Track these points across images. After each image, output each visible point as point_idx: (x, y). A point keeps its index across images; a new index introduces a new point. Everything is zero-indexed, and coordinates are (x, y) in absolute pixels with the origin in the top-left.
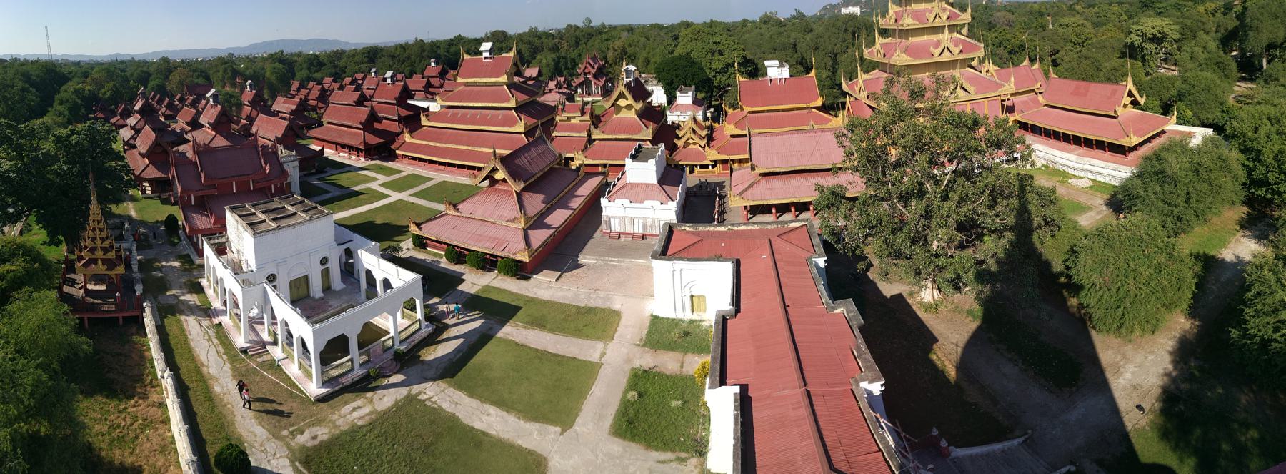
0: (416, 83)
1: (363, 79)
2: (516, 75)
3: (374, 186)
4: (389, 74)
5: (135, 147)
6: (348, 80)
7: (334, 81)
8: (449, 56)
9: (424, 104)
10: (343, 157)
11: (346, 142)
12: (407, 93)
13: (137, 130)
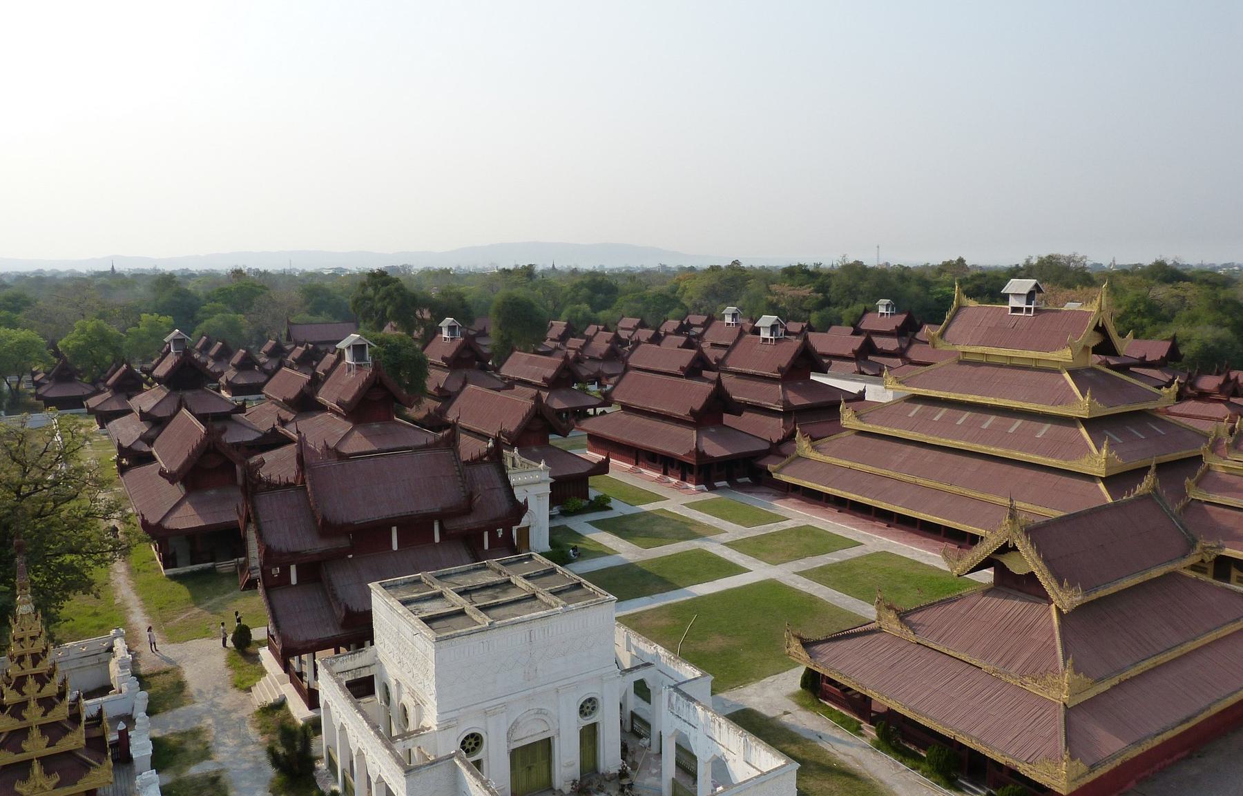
0: (838, 340)
1: (706, 325)
4: (766, 321)
5: (150, 458)
6: (672, 324)
7: (642, 325)
9: (853, 387)
10: (648, 479)
13: (156, 422)
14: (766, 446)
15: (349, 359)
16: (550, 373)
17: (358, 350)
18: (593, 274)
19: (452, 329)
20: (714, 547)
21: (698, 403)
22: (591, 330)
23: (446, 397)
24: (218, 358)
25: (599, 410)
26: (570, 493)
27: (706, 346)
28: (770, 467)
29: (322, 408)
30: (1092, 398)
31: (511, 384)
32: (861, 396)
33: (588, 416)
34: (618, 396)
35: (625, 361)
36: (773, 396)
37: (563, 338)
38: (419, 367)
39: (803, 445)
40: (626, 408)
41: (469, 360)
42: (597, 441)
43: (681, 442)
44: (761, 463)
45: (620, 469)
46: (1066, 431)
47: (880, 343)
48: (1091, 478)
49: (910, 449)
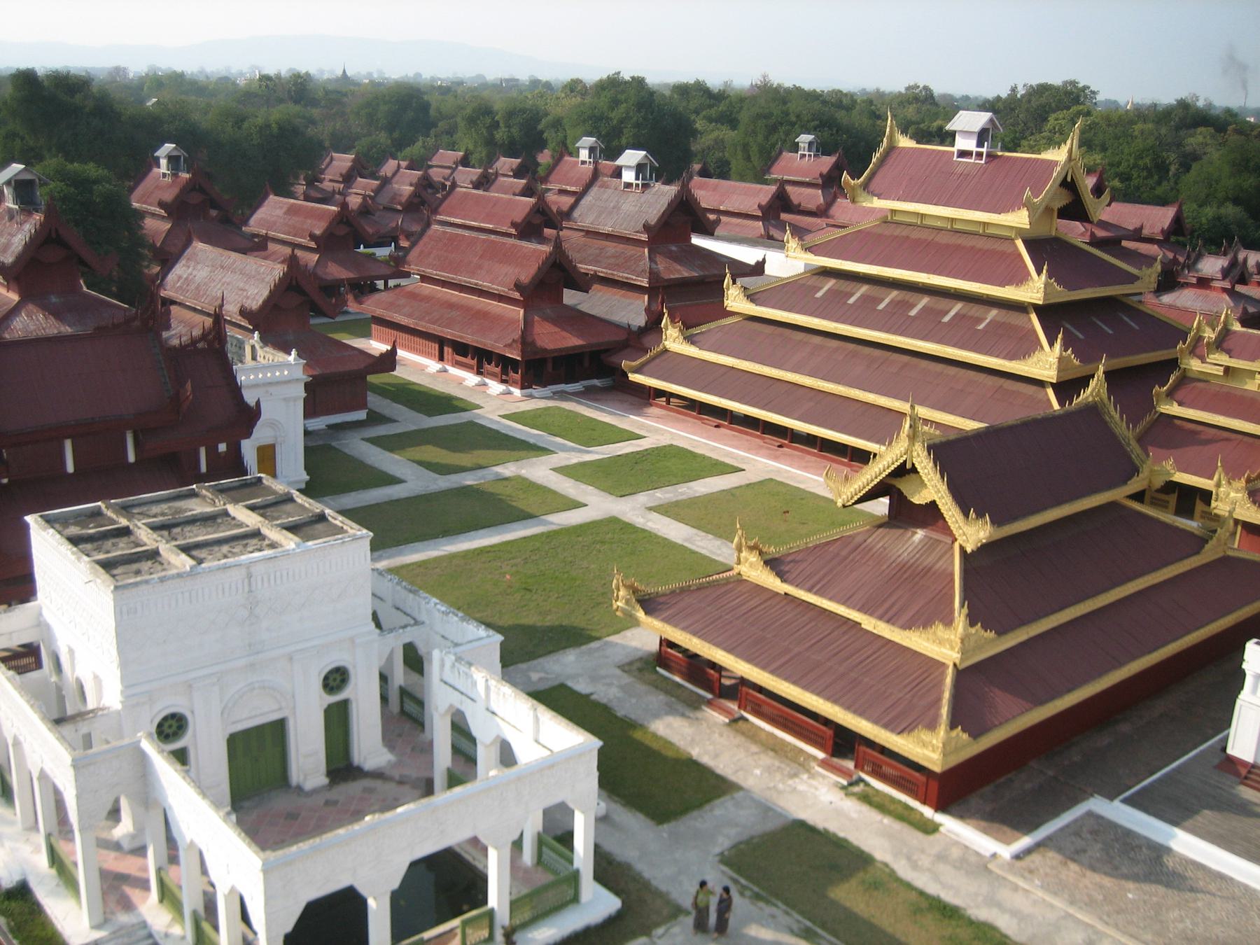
2: (1065, 213)
4: (632, 157)
8: (849, 134)
11: (469, 338)
12: (686, 217)
14: (622, 337)
20: (539, 471)
25: (391, 283)
28: (625, 364)
30: (1050, 276)
33: (374, 289)
37: (348, 179)
44: (614, 359)
46: (1015, 318)
48: (1040, 384)
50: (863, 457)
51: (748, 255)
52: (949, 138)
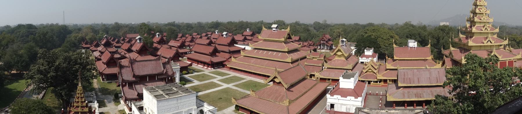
0: (238, 37)
1: (211, 34)
3: (215, 81)
6: (204, 34)
7: (198, 34)
8: (256, 29)
10: (200, 67)
14: (225, 60)
15: (138, 41)
16: (179, 45)
17: (140, 39)
18: (187, 24)
19: (158, 35)
21: (211, 51)
22: (187, 36)
23: (157, 49)
24: (113, 41)
26: (184, 69)
27: (212, 39)
29: (132, 51)
31: (171, 47)
32: (244, 49)
34: (193, 49)
35: (194, 42)
36: (227, 49)
37: (181, 37)
38: (153, 43)
39: (233, 59)
40: (195, 52)
41: (162, 42)
42: (189, 59)
43: (207, 59)
44: (224, 63)
45: (195, 66)
47: (247, 37)
49: (255, 59)
50: (268, 77)
51: (243, 47)
52: (272, 28)
